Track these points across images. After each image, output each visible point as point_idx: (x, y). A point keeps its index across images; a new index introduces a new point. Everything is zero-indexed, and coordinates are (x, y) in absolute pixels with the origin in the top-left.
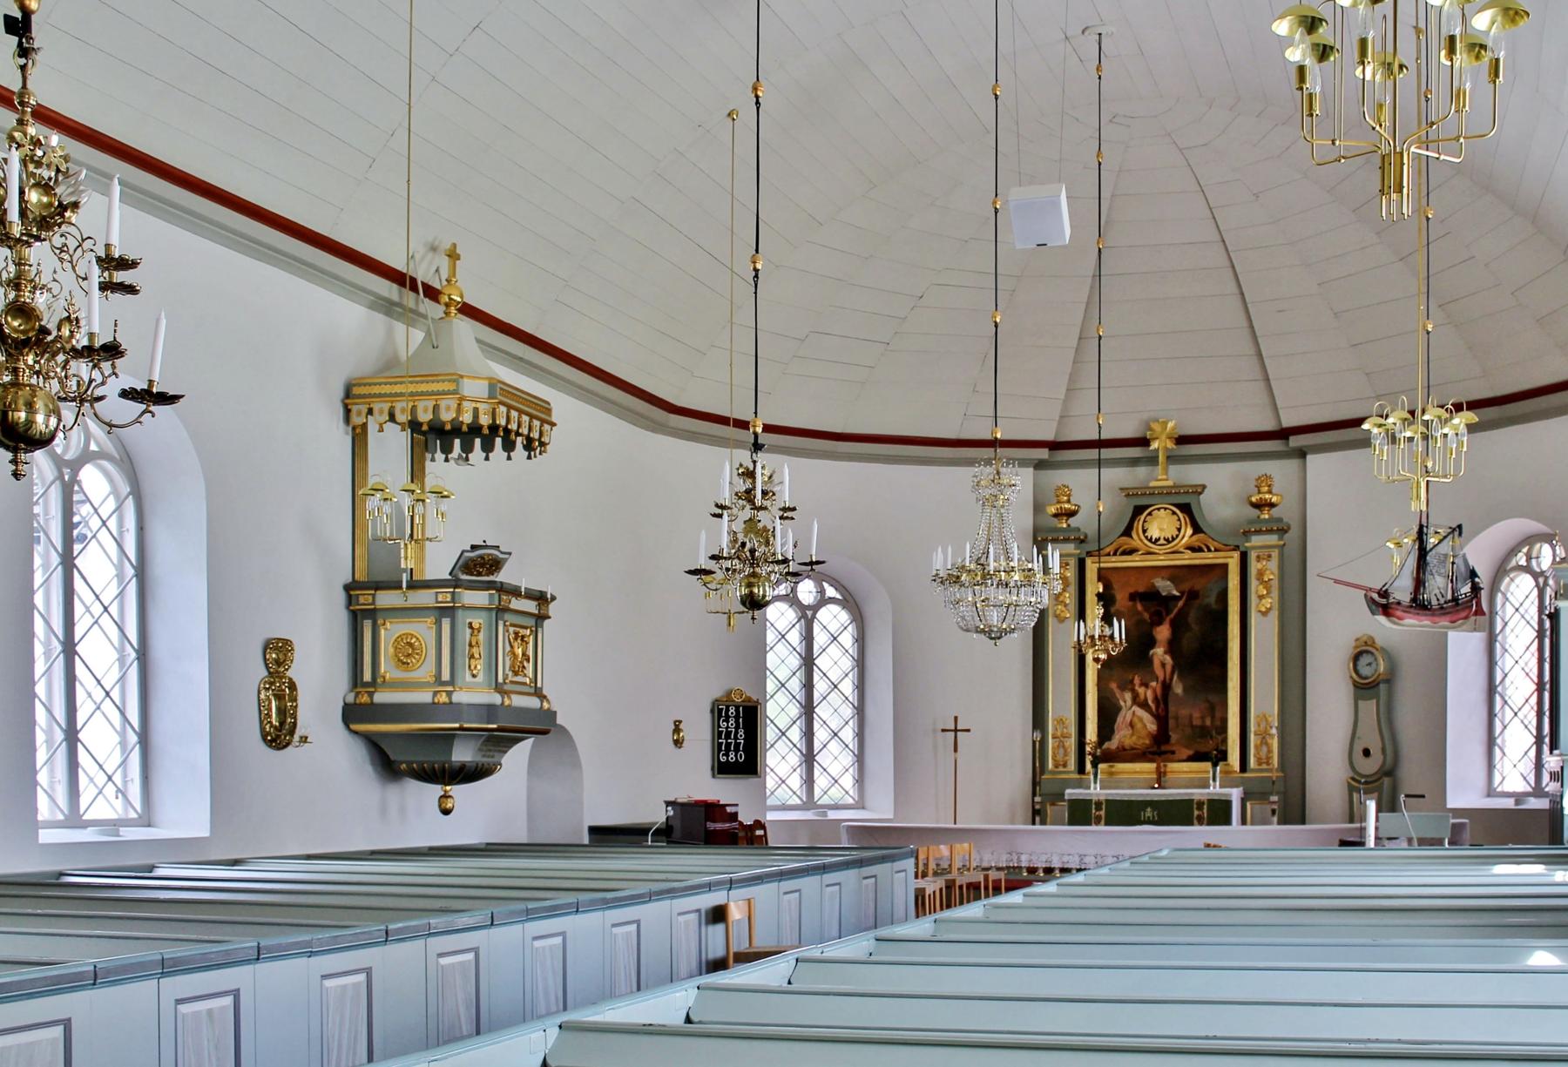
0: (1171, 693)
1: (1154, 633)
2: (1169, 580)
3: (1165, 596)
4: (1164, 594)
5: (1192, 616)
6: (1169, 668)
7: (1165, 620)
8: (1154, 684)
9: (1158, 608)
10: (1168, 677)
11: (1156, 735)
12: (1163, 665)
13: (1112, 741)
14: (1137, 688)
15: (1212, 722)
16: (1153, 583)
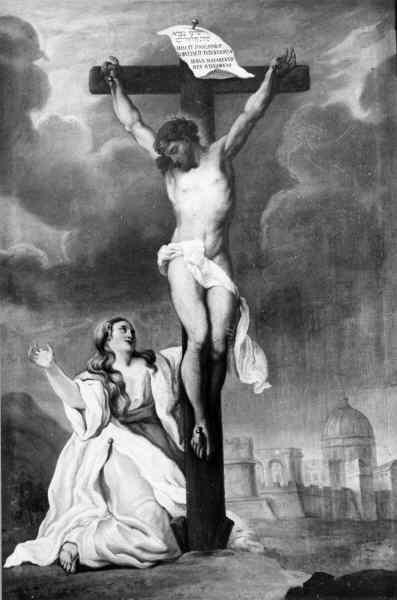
0: (229, 378)
1: (170, 189)
2: (214, 29)
3: (198, 79)
4: (199, 73)
5: (295, 137)
6: (220, 305)
7: (205, 150)
8: (173, 353)
10: (218, 332)
12: (204, 294)
13: (39, 540)
14: (119, 364)
15: (364, 477)
16: (167, 40)
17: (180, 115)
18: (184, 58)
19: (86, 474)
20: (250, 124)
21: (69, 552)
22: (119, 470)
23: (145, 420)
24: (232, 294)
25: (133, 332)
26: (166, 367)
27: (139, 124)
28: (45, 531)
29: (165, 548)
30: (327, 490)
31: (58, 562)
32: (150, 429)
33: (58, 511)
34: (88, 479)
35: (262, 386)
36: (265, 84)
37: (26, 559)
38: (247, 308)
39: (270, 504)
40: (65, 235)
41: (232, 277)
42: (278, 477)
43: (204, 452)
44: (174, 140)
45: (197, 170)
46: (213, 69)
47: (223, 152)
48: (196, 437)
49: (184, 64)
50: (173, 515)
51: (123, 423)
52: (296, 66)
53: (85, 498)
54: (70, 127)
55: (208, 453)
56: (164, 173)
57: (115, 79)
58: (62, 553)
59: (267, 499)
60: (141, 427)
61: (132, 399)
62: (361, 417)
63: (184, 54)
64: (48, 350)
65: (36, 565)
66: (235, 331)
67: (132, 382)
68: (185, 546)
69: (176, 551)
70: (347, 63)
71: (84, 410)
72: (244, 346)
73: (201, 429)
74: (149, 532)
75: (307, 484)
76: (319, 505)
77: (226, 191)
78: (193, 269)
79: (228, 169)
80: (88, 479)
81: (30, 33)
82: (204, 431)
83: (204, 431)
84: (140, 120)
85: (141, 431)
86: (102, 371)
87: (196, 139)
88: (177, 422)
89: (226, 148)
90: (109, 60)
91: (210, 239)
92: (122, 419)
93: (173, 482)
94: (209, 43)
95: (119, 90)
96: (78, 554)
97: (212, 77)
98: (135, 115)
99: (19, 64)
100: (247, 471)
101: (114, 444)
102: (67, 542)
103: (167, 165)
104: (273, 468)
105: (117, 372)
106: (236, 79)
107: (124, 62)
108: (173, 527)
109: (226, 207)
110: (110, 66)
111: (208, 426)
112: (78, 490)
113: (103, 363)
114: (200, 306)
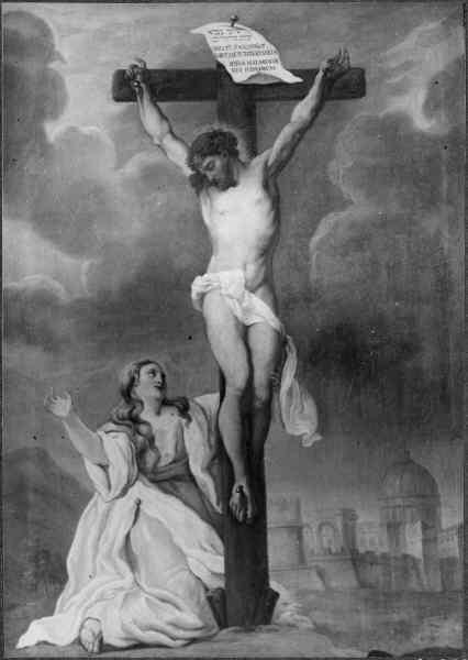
0: (273, 427)
2: (254, 27)
4: (239, 77)
6: (264, 346)
7: (245, 165)
9: (225, 129)
10: (260, 377)
11: (223, 593)
12: (244, 332)
13: (57, 616)
14: (147, 414)
16: (202, 39)
17: (216, 127)
18: (220, 60)
19: (110, 541)
20: (298, 136)
21: (91, 630)
22: (148, 537)
23: (176, 478)
24: (275, 331)
25: (163, 376)
26: (201, 418)
27: (169, 136)
28: (62, 605)
29: (199, 623)
30: (384, 556)
31: (78, 641)
32: (183, 488)
33: (78, 581)
34: (113, 544)
35: (311, 438)
36: (314, 91)
37: (42, 639)
38: (293, 348)
39: (321, 574)
40: (86, 264)
41: (277, 313)
42: (330, 542)
43: (245, 515)
44: (211, 154)
45: (239, 187)
46: (255, 73)
47: (266, 168)
48: (236, 497)
49: (220, 66)
50: (210, 587)
51: (153, 481)
52: (349, 68)
53: (108, 567)
54: (91, 141)
55: (249, 516)
56: (198, 193)
57: (143, 85)
58: (84, 631)
59: (316, 567)
60: (172, 485)
61: (163, 454)
62: (424, 473)
63: (221, 56)
64: (66, 398)
65: (54, 645)
66: (281, 374)
67: (163, 433)
68: (223, 624)
69: (213, 627)
70: (407, 65)
71: (108, 466)
72: (290, 392)
73: (241, 488)
74: (179, 601)
75: (362, 550)
76: (375, 574)
77: (269, 213)
78: (229, 302)
79: (273, 189)
80: (113, 544)
81: (45, 31)
82: (245, 490)
83: (245, 490)
84: (171, 132)
85: (171, 489)
86: (128, 422)
87: (235, 154)
88: (214, 479)
89: (270, 163)
90: (137, 63)
91: (252, 268)
92: (152, 476)
93: (209, 548)
94: (249, 43)
95: (146, 96)
96: (101, 632)
97: (254, 81)
98: (165, 126)
99: (30, 67)
100: (295, 536)
101: (141, 507)
102: (89, 618)
103: (200, 183)
104: (324, 531)
105: (145, 423)
106: (281, 84)
107: (155, 62)
108: (210, 599)
109: (270, 232)
110: (136, 70)
111: (250, 486)
112: (99, 557)
113: (131, 412)
114: (241, 346)
